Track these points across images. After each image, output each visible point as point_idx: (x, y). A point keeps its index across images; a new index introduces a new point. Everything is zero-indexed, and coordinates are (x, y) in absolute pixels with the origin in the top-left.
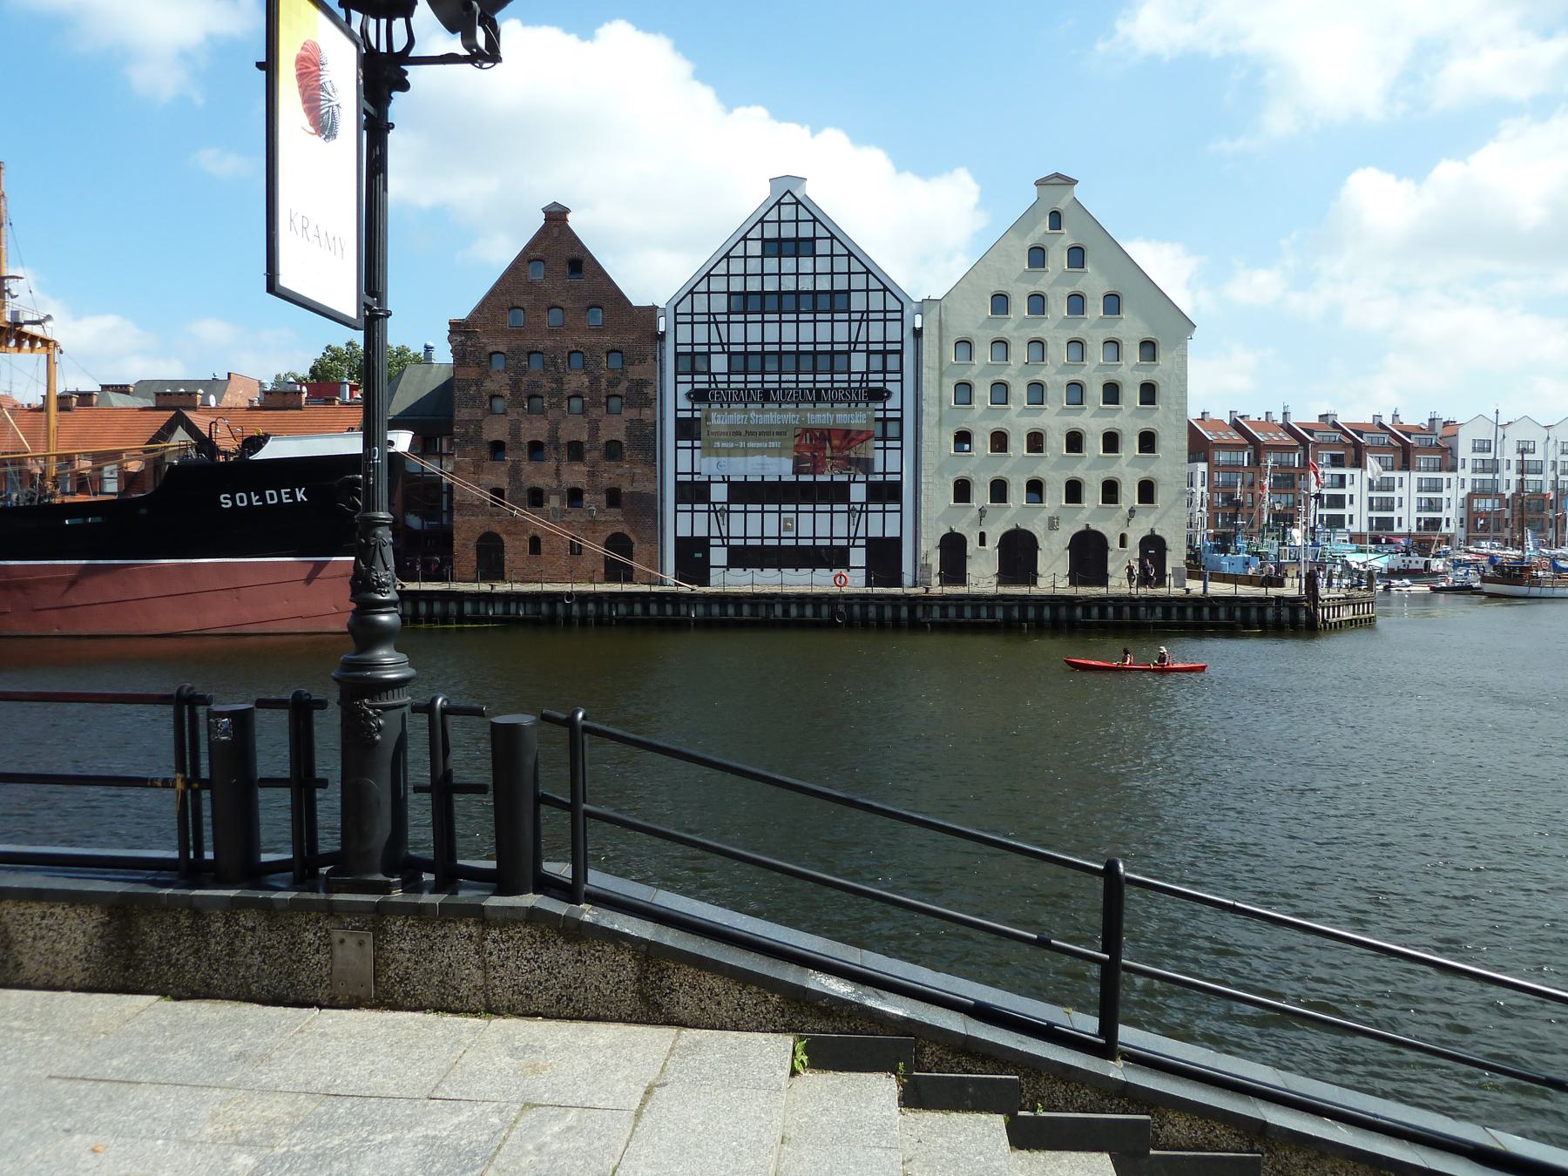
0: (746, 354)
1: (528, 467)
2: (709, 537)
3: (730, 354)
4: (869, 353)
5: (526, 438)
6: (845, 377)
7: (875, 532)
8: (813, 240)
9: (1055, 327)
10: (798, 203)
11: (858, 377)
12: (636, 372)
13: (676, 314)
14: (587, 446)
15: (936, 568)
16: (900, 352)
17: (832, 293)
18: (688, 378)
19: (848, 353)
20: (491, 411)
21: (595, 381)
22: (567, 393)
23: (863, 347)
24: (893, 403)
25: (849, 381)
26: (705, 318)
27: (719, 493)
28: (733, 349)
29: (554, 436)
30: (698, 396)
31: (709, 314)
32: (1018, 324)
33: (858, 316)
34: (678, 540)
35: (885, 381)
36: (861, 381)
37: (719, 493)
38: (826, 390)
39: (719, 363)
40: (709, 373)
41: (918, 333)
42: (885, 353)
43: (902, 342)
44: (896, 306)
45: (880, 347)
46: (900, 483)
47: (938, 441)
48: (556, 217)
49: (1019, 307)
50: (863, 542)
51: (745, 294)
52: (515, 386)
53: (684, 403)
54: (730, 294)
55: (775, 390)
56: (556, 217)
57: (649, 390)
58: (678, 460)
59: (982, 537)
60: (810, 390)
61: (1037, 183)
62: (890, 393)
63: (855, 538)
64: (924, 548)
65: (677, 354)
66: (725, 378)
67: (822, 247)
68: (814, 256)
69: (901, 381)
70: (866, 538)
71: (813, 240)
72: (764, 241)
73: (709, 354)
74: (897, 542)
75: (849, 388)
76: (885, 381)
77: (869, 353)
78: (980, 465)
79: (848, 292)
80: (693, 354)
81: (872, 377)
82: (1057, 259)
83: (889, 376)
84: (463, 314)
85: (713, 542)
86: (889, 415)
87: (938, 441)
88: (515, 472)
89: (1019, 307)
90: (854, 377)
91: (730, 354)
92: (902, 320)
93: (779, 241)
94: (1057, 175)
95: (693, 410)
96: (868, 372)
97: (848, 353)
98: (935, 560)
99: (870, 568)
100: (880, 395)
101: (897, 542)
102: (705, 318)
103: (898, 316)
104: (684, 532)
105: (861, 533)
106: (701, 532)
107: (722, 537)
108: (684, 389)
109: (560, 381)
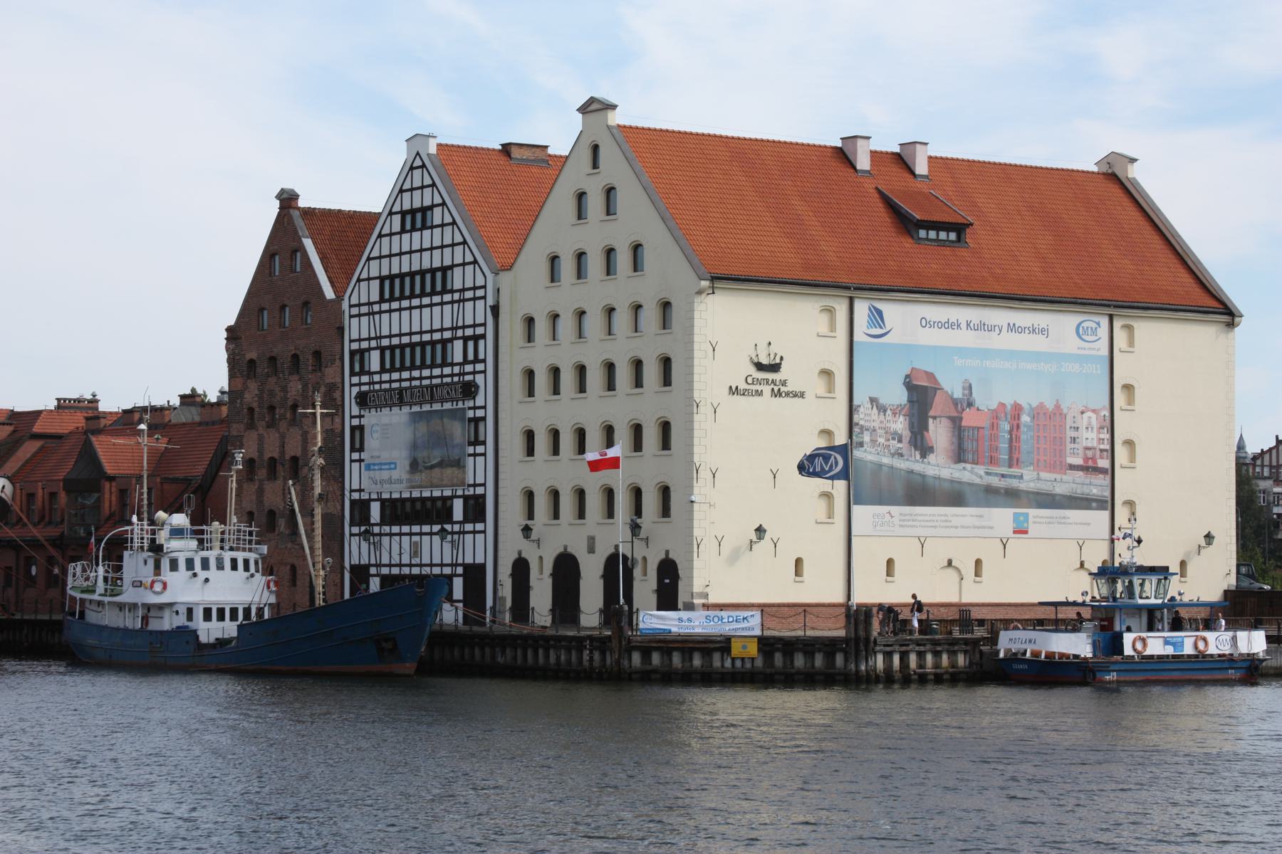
0: (392, 348)
1: (268, 486)
2: (370, 565)
3: (383, 350)
4: (465, 339)
5: (267, 455)
7: (469, 560)
8: (431, 208)
9: (596, 291)
10: (423, 166)
11: (457, 369)
12: (330, 374)
13: (351, 306)
14: (301, 463)
15: (509, 603)
16: (483, 336)
17: (444, 270)
18: (355, 380)
19: (451, 340)
20: (251, 426)
21: (305, 386)
22: (290, 403)
23: (460, 333)
24: (480, 401)
25: (452, 375)
26: (364, 309)
27: (375, 511)
28: (385, 342)
29: (283, 453)
30: (363, 400)
31: (370, 304)
32: (568, 296)
33: (456, 296)
34: (352, 567)
35: (474, 373)
36: (459, 375)
37: (375, 511)
39: (374, 361)
40: (370, 373)
41: (495, 310)
42: (476, 338)
43: (484, 325)
44: (480, 282)
45: (469, 332)
46: (483, 496)
47: (512, 444)
48: (287, 200)
49: (567, 267)
50: (460, 570)
51: (392, 278)
52: (261, 397)
53: (356, 411)
54: (382, 279)
55: (406, 389)
56: (287, 200)
57: (337, 395)
59: (541, 558)
60: (427, 387)
61: (584, 110)
62: (477, 387)
63: (457, 565)
64: (500, 577)
65: (352, 353)
66: (376, 378)
68: (432, 227)
69: (484, 372)
70: (466, 567)
71: (431, 208)
72: (403, 214)
73: (369, 349)
74: (482, 567)
75: (453, 383)
76: (474, 373)
77: (465, 339)
78: (544, 472)
79: (451, 267)
80: (362, 352)
81: (469, 368)
82: (595, 203)
83: (480, 367)
84: (232, 322)
85: (373, 570)
86: (480, 413)
87: (512, 444)
88: (260, 492)
89: (567, 267)
90: (457, 369)
91: (383, 350)
92: (484, 298)
94: (592, 100)
95: (360, 417)
97: (451, 340)
98: (507, 591)
99: (466, 601)
100: (469, 390)
101: (482, 567)
102: (364, 309)
103: (480, 293)
104: (355, 561)
105: (460, 561)
106: (364, 561)
107: (376, 565)
108: (355, 390)
109: (284, 389)
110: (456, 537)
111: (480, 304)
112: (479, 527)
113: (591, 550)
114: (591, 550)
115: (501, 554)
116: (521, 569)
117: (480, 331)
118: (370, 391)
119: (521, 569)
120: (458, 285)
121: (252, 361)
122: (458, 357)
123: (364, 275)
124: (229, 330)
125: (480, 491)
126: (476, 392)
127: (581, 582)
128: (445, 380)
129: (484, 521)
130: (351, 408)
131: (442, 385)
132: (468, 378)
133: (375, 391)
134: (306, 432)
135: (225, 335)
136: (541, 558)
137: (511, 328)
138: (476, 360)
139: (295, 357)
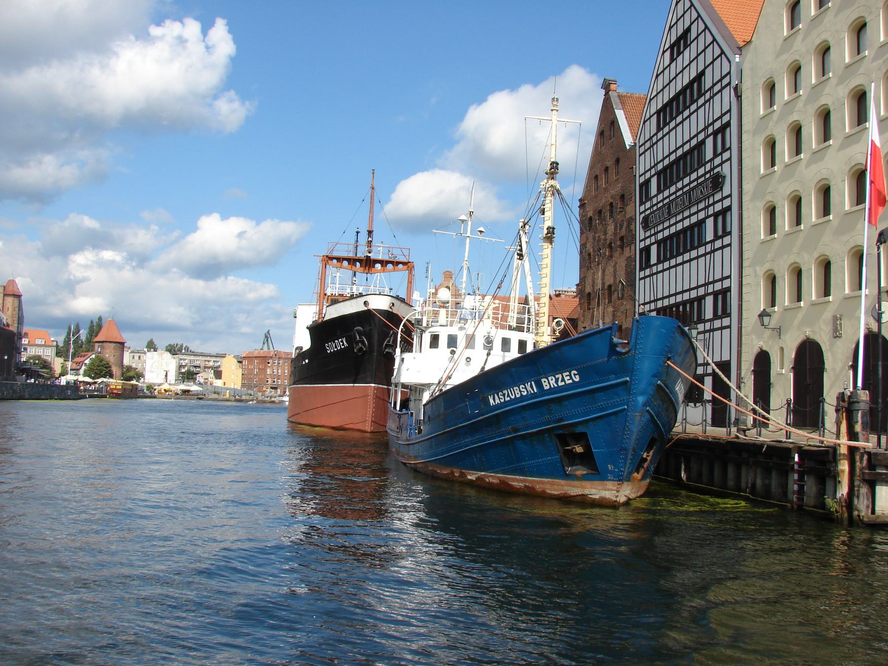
6: (701, 171)
12: (629, 209)
22: (608, 242)
23: (710, 130)
24: (726, 191)
38: (693, 189)
54: (658, 112)
57: (632, 227)
58: (644, 291)
59: (782, 349)
67: (693, 34)
86: (726, 203)
93: (677, 42)
95: (644, 239)
96: (716, 155)
100: (717, 182)
102: (648, 145)
110: (707, 335)
111: (726, 92)
112: (726, 322)
113: (836, 333)
114: (836, 333)
115: (744, 349)
116: (763, 361)
117: (725, 119)
118: (651, 213)
119: (763, 361)
120: (708, 84)
121: (591, 218)
122: (709, 154)
123: (648, 116)
124: (580, 200)
125: (726, 284)
126: (723, 183)
127: (825, 374)
128: (699, 181)
129: (729, 315)
130: (640, 233)
131: (698, 184)
132: (716, 171)
133: (654, 212)
134: (616, 263)
135: (578, 204)
136: (782, 349)
137: (755, 105)
138: (724, 150)
139: (611, 205)
